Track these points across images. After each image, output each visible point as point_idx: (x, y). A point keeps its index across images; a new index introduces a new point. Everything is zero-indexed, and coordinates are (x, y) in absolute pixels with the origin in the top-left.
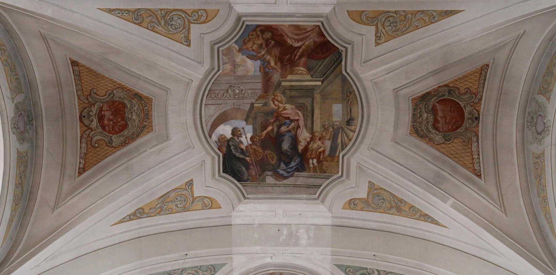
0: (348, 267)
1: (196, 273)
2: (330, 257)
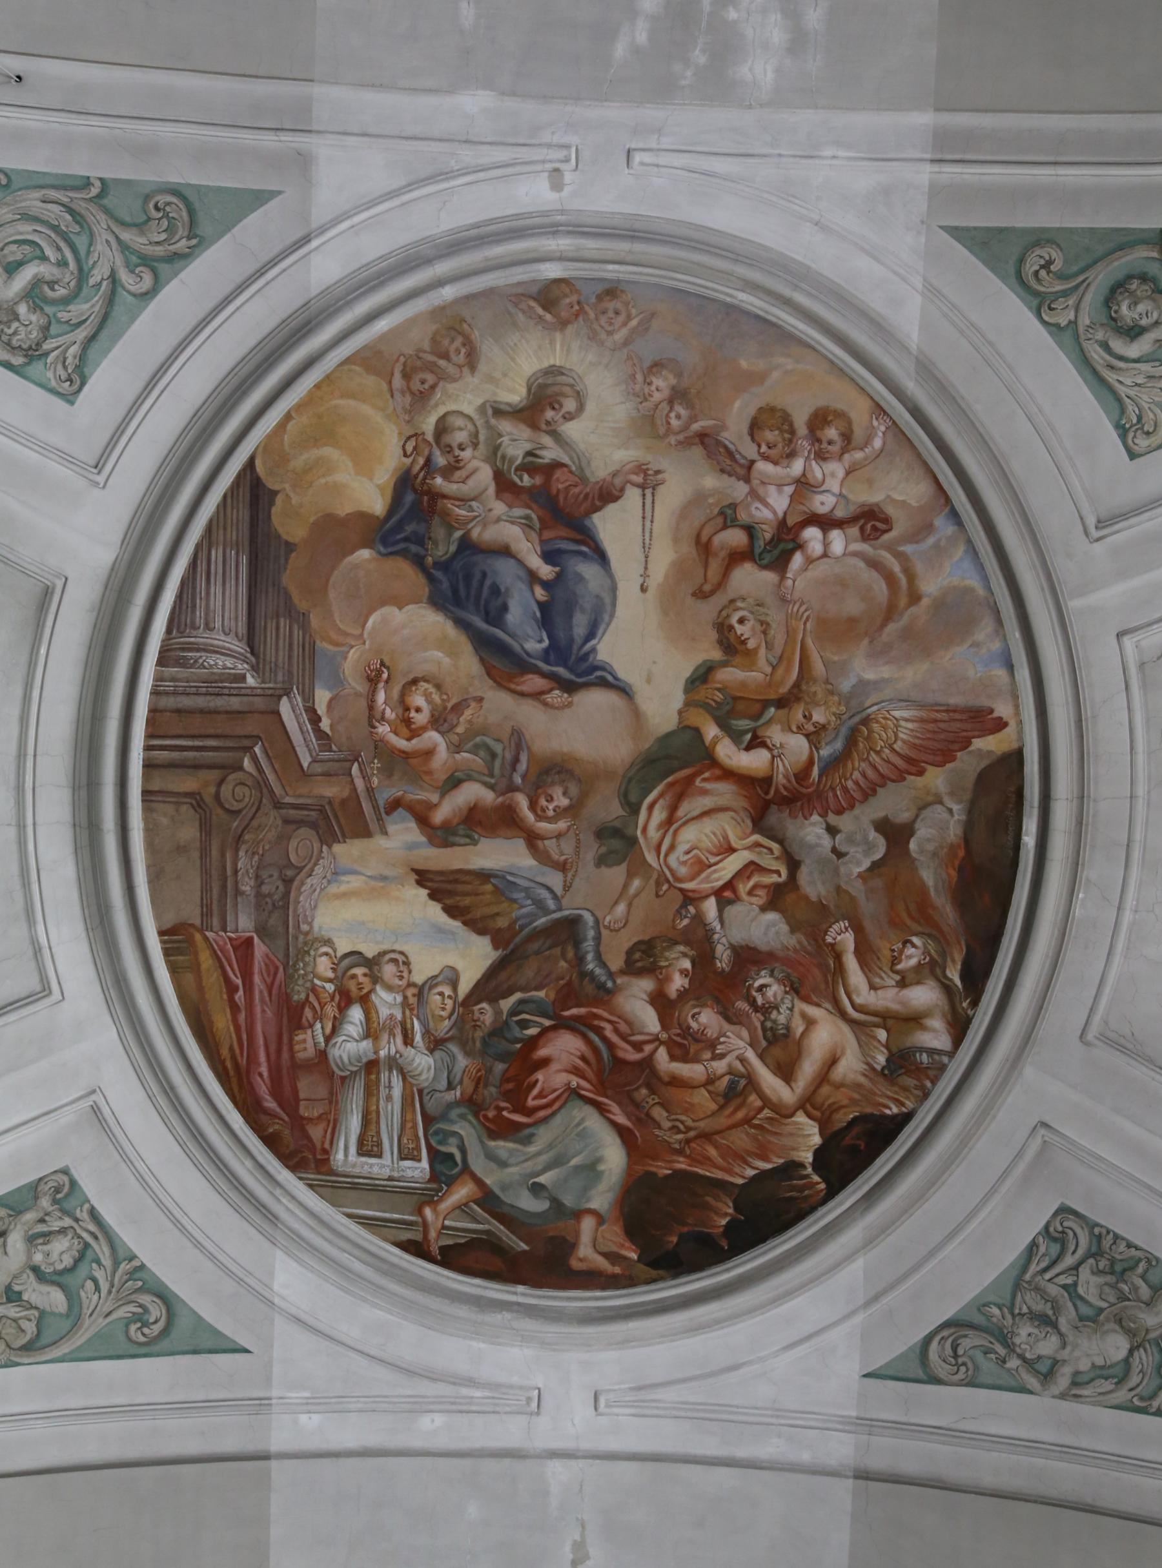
0: (1040, 238)
1: (77, 228)
2: (924, 174)
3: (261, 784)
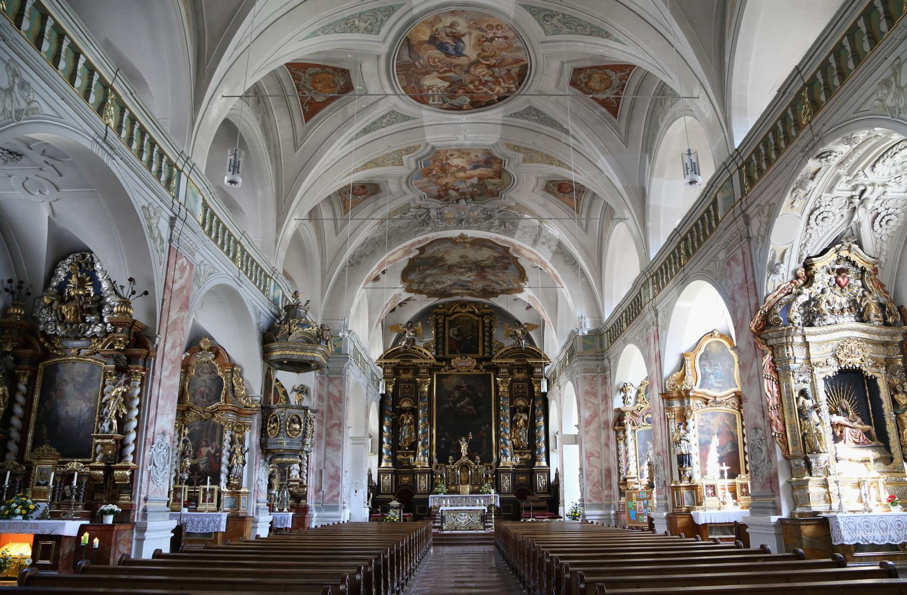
3: (414, 71)
